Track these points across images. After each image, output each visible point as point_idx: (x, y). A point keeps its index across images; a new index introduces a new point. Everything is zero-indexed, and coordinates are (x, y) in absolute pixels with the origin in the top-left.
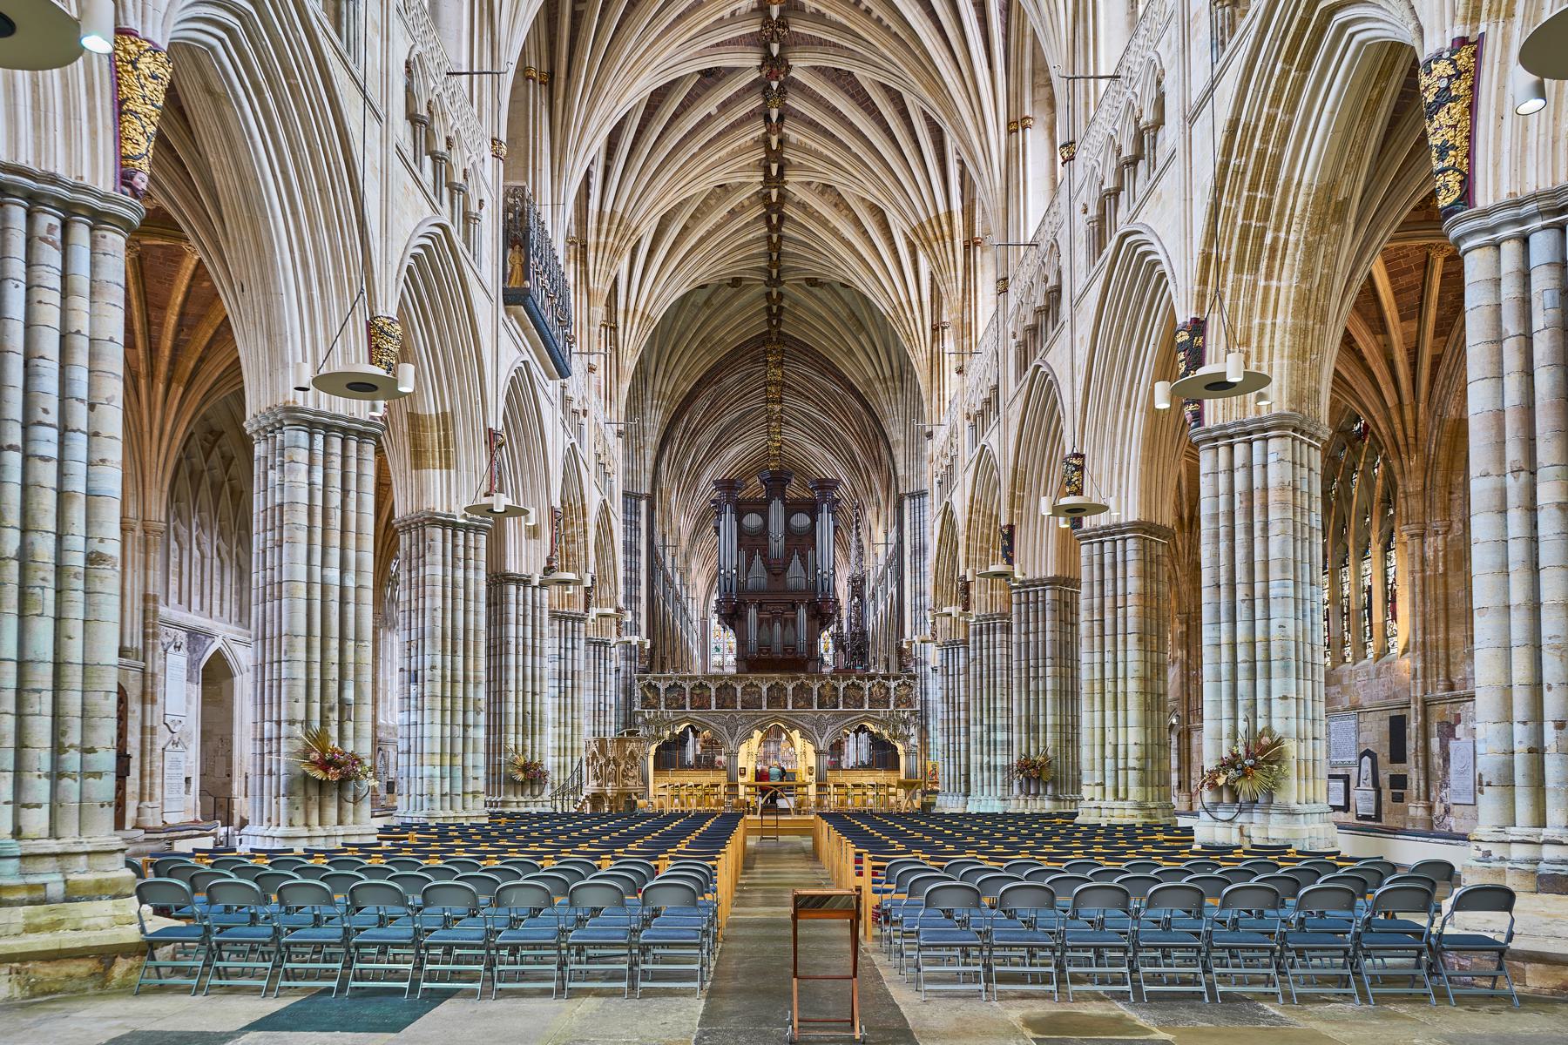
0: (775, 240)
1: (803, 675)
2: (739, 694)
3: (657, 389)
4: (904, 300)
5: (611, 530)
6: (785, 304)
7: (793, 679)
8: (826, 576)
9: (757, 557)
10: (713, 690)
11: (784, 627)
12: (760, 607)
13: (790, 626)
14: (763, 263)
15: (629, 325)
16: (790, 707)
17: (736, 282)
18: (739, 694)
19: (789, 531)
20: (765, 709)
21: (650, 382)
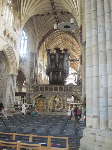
0: (52, 3)
1: (61, 85)
2: (49, 88)
3: (38, 35)
4: (74, 8)
5: (14, 53)
6: (59, 19)
7: (59, 86)
8: (65, 66)
9: (54, 63)
10: (44, 88)
11: (57, 76)
12: (53, 72)
13: (58, 76)
14: (52, 9)
15: (23, 16)
16: (58, 91)
17: (49, 14)
18: (49, 88)
19: (59, 59)
20: (54, 91)
21: (36, 34)
